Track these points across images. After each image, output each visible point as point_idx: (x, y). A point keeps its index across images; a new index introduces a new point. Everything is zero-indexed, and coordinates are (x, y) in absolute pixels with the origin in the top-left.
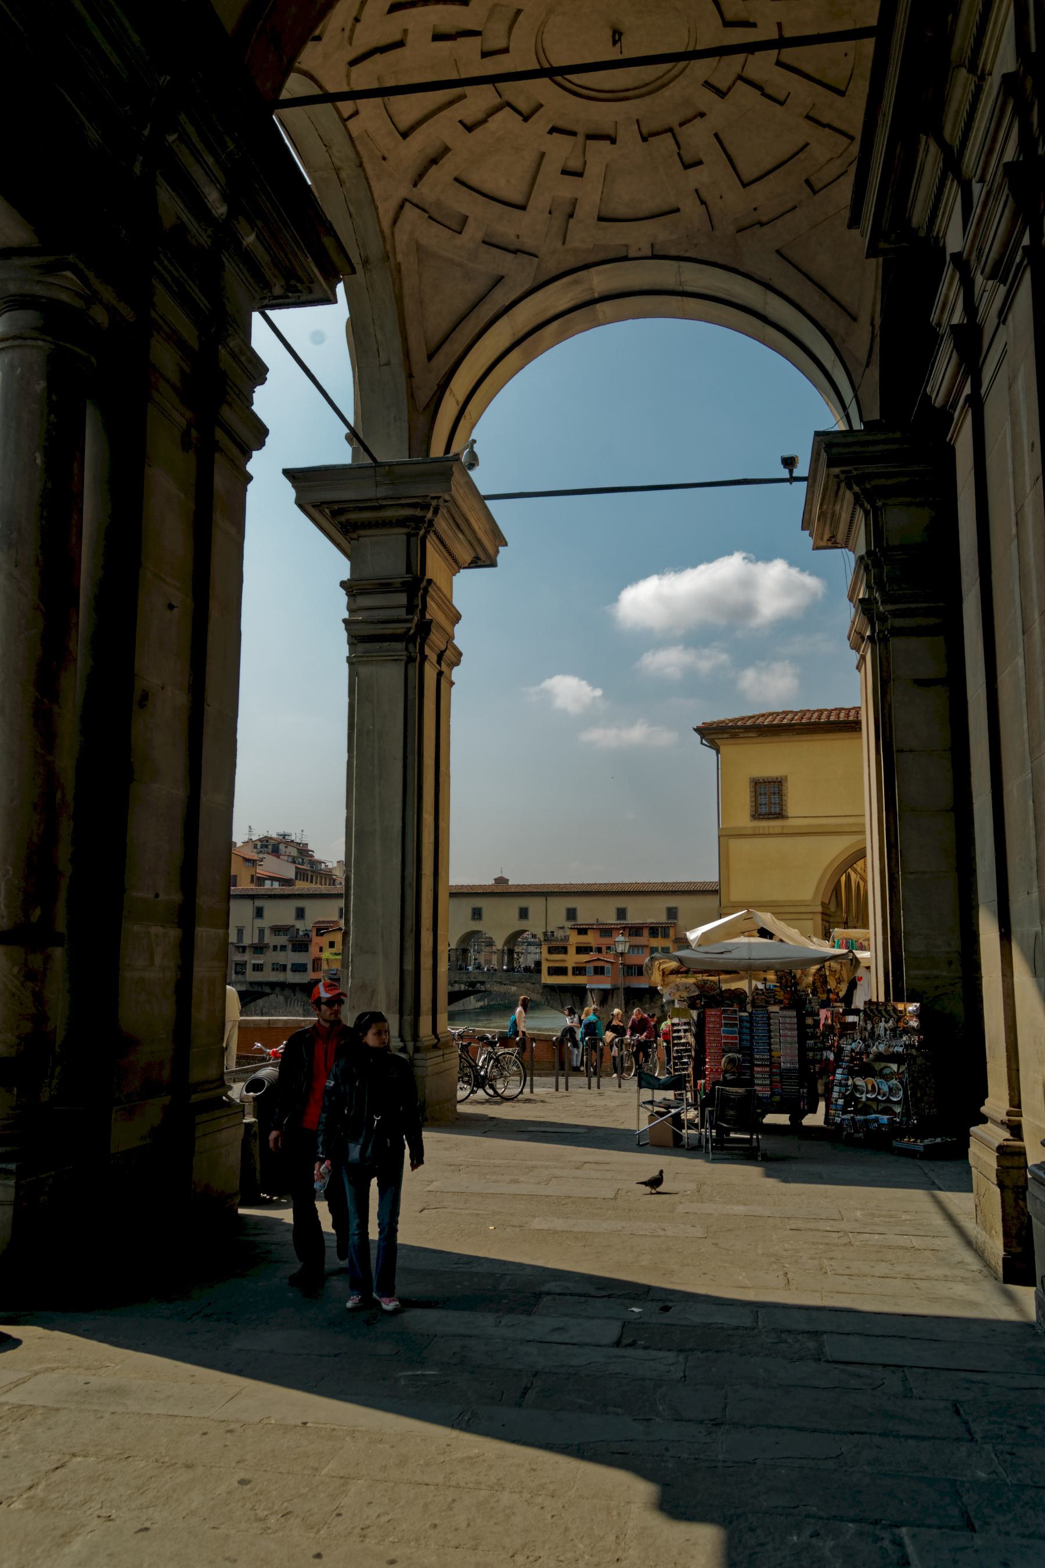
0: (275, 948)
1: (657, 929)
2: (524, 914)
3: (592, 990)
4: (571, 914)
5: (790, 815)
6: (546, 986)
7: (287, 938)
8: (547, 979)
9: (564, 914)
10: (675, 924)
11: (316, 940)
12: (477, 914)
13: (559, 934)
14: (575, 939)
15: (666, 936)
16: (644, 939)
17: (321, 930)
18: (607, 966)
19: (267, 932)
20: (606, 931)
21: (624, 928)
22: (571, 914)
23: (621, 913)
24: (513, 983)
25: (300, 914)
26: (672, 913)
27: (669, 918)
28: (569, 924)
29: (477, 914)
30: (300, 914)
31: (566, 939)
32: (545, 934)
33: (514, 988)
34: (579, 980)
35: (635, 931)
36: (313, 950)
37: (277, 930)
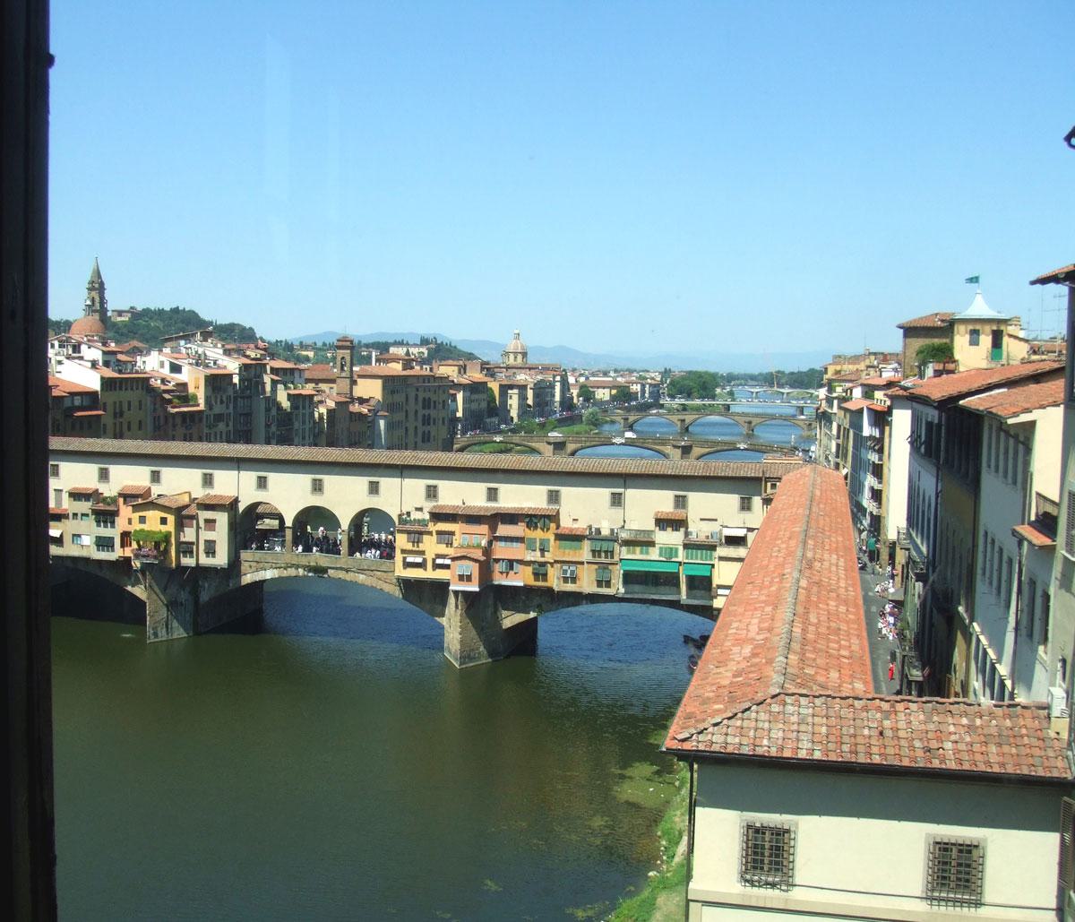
0: (75, 515)
1: (535, 516)
2: (374, 489)
3: (456, 593)
4: (432, 493)
5: (797, 880)
6: (398, 579)
7: (89, 504)
9: (423, 492)
11: (125, 511)
12: (317, 487)
13: (416, 515)
15: (545, 528)
16: (518, 530)
17: (127, 497)
19: (65, 496)
20: (472, 519)
22: (432, 493)
23: (492, 495)
25: (104, 475)
26: (554, 497)
29: (317, 487)
30: (104, 475)
32: (400, 516)
33: (361, 578)
34: (441, 575)
35: (511, 518)
36: (121, 524)
37: (76, 496)
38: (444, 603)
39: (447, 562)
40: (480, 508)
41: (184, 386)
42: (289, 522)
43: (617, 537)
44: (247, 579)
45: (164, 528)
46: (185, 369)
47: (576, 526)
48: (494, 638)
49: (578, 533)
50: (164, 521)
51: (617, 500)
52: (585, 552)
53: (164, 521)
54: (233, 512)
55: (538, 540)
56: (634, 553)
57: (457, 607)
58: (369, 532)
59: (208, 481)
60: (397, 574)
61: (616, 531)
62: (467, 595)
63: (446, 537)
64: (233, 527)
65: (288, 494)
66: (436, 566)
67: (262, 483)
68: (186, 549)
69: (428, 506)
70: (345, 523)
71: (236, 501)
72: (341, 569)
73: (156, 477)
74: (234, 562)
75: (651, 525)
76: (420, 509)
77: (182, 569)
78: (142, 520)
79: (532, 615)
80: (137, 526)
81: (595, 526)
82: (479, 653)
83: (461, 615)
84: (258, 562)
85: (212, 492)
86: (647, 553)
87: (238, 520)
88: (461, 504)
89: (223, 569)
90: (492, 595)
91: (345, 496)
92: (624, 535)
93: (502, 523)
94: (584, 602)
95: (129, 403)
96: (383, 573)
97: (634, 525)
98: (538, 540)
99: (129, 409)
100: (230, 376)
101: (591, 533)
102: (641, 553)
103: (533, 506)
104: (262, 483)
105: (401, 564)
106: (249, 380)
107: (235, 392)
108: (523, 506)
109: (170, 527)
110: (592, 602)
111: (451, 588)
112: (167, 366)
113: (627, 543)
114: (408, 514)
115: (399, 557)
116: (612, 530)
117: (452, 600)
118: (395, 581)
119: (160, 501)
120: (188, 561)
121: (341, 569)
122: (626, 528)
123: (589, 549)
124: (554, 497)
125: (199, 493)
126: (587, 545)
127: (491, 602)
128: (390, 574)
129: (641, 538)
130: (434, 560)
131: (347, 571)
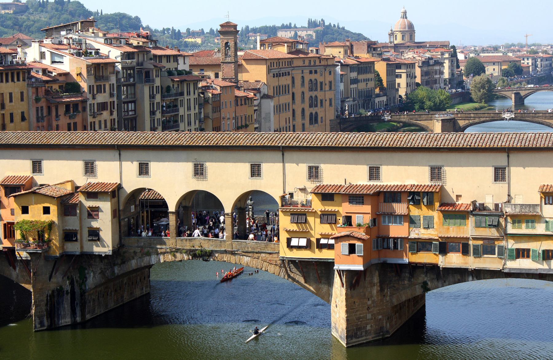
1: (418, 193)
2: (256, 171)
6: (283, 261)
8: (285, 253)
10: (442, 188)
14: (318, 206)
18: (358, 244)
20: (356, 197)
21: (378, 194)
22: (314, 173)
23: (374, 173)
24: (246, 253)
26: (436, 173)
27: (432, 178)
28: (311, 186)
31: (308, 203)
32: (283, 198)
34: (326, 254)
38: (330, 283)
39: (332, 242)
40: (363, 187)
41: (67, 75)
42: (172, 207)
43: (502, 211)
44: (134, 264)
45: (46, 218)
46: (67, 59)
47: (460, 202)
48: (380, 317)
49: (462, 209)
50: (46, 211)
51: (500, 174)
52: (468, 229)
53: (46, 211)
54: (116, 199)
55: (422, 219)
56: (521, 228)
57: (343, 286)
58: (255, 216)
59: (90, 169)
60: (282, 255)
61: (500, 206)
62: (349, 272)
63: (328, 218)
64: (116, 213)
65: (170, 181)
66: (321, 247)
67: (144, 170)
68: (69, 236)
69: (311, 186)
70: (228, 208)
71: (119, 187)
72: (226, 252)
73: (37, 167)
74: (119, 248)
75: (536, 198)
76: (303, 190)
77: (66, 257)
78: (25, 210)
79: (418, 291)
80: (19, 217)
81: (479, 202)
82: (366, 331)
83: (346, 294)
84: (142, 248)
85: (93, 180)
86: (533, 228)
87: (121, 208)
88: (343, 184)
89: (107, 256)
90: (377, 273)
91: (228, 181)
92: (508, 210)
93: (385, 202)
94: (471, 278)
95: (11, 94)
96: (267, 255)
97: (518, 200)
98: (422, 219)
99: (11, 101)
100: (113, 64)
101: (475, 208)
102: (527, 227)
103: (416, 184)
104: (144, 170)
105: (285, 245)
106: (133, 68)
107: (118, 80)
108: (406, 184)
109: (53, 216)
110: (479, 278)
111: (336, 267)
112: (48, 55)
113: (513, 216)
114: (291, 195)
115: (283, 236)
116: (497, 205)
117: (337, 279)
118: (279, 262)
119: (42, 191)
120: (73, 248)
121: (226, 252)
122: (513, 202)
123: (474, 225)
124: (436, 173)
125: (82, 181)
126: (471, 220)
127: (376, 280)
128: (275, 256)
129: (526, 211)
130: (318, 240)
131: (233, 253)
